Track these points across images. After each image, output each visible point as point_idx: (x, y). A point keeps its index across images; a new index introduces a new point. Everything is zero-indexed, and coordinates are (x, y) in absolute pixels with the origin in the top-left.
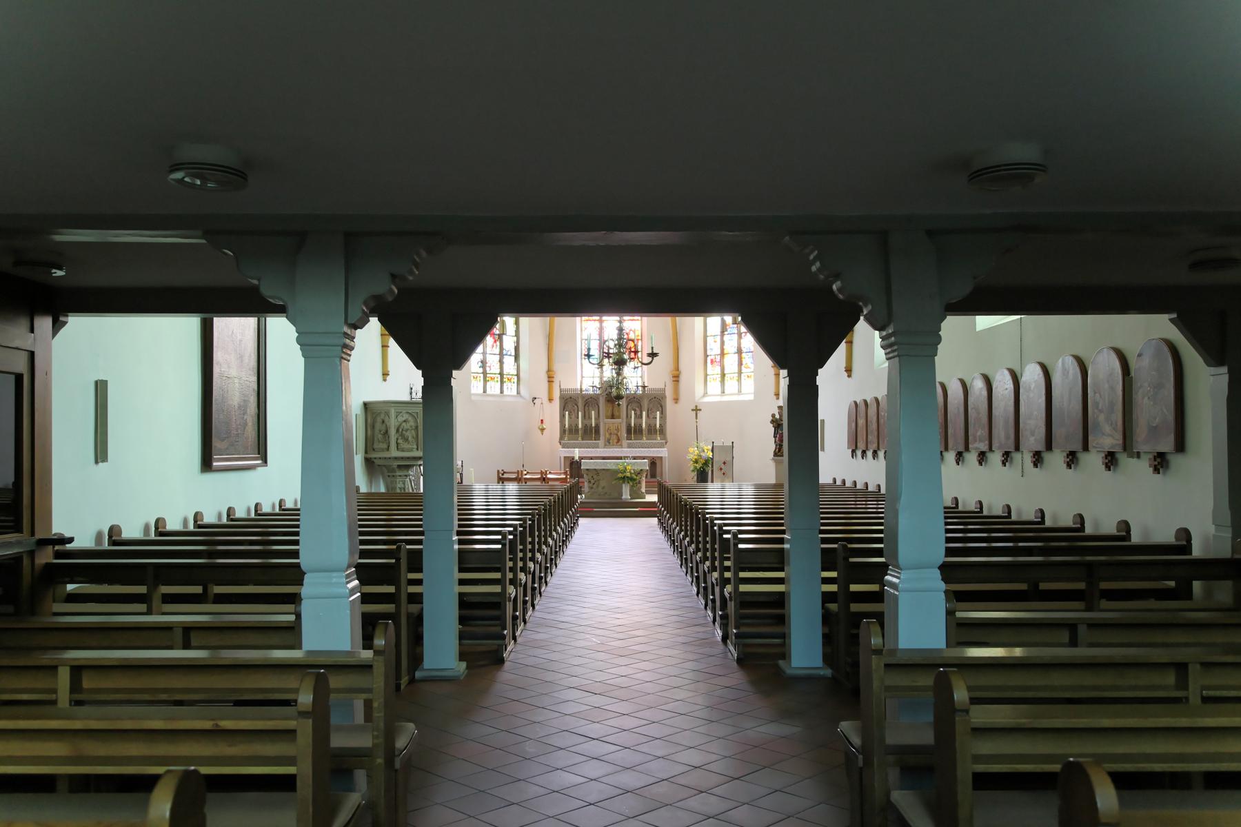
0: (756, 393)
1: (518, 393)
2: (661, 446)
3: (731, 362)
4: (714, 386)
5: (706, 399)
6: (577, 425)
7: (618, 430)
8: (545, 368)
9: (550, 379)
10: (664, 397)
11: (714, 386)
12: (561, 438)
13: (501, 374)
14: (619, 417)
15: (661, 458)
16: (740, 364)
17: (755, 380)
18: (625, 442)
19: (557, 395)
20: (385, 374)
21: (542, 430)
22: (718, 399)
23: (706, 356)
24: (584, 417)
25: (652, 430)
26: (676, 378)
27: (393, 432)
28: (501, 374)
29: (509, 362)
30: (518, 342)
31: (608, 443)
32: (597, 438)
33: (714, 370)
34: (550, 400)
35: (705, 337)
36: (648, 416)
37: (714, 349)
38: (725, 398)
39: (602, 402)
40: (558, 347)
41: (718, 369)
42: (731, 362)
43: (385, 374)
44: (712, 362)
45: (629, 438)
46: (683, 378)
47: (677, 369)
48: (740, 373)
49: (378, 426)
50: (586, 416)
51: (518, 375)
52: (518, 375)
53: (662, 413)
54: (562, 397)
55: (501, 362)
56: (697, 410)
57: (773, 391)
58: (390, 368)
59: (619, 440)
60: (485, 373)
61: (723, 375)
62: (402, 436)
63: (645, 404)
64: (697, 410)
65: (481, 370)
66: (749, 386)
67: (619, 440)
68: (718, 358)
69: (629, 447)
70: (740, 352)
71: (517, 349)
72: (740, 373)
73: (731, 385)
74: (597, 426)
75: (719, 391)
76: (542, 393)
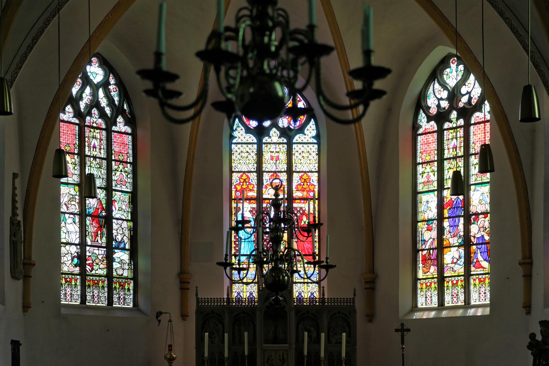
0: (492, 305)
1: (135, 305)
3: (452, 256)
5: (417, 315)
6: (222, 353)
8: (176, 269)
10: (352, 311)
11: (427, 299)
13: (109, 276)
14: (285, 341)
16: (468, 262)
17: (490, 284)
23: (416, 251)
24: (232, 342)
26: (371, 284)
28: (109, 276)
29: (122, 256)
33: (426, 273)
34: (184, 316)
35: (415, 222)
36: (328, 340)
38: (444, 314)
39: (259, 317)
41: (433, 270)
42: (452, 256)
46: (382, 286)
47: (372, 269)
48: (468, 275)
50: (236, 341)
51: (135, 279)
53: (348, 336)
54: (199, 311)
56: (403, 330)
57: (520, 300)
60: (83, 274)
61: (441, 279)
65: (77, 270)
66: (481, 295)
68: (434, 253)
70: (467, 243)
71: (133, 239)
72: (468, 275)
73: (453, 297)
75: (435, 302)
76: (171, 304)
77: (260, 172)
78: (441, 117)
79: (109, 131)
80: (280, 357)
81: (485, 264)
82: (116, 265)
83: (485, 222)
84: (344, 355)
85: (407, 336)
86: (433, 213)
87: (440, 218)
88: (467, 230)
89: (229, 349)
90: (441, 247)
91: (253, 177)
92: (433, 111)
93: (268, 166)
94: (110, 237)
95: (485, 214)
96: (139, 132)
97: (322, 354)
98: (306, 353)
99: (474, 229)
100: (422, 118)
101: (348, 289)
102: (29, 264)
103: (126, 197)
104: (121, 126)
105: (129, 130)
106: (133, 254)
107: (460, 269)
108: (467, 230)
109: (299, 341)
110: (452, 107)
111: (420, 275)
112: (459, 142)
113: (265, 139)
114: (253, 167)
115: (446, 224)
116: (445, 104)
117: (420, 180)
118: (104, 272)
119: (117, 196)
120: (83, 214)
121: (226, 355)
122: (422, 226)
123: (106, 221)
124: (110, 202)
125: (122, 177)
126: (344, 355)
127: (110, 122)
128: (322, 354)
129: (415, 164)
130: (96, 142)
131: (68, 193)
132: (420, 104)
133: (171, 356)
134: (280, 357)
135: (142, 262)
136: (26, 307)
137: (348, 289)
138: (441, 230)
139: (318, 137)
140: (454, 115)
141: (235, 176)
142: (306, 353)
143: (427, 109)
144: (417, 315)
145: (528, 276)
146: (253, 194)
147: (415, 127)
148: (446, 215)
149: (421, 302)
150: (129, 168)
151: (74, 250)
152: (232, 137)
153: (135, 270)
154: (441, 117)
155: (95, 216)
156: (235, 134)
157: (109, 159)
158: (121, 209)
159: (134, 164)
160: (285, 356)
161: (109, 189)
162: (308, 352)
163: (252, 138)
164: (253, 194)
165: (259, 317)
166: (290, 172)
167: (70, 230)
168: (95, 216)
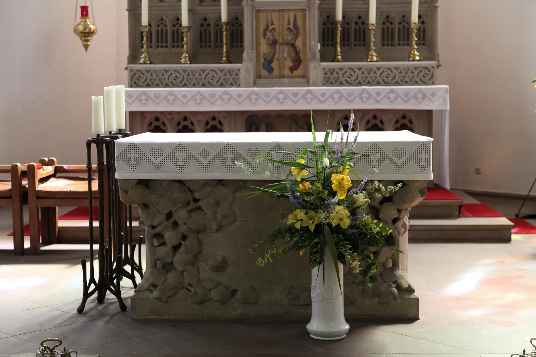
2: (427, 77)
7: (295, 30)
12: (133, 58)
15: (429, 113)
18: (317, 68)
21: (86, 35)
25: (397, 34)
31: (267, 71)
32: (235, 56)
45: (328, 55)
59: (297, 62)
67: (297, 62)
69: (330, 79)
74: (236, 23)
80: (289, 24)
84: (415, 18)
89: (190, 10)
97: (373, 18)
98: (339, 16)
121: (185, 21)
126: (415, 18)
128: (373, 18)
133: (86, 26)
134: (289, 24)
142: (339, 16)
160: (299, 23)
162: (344, 17)
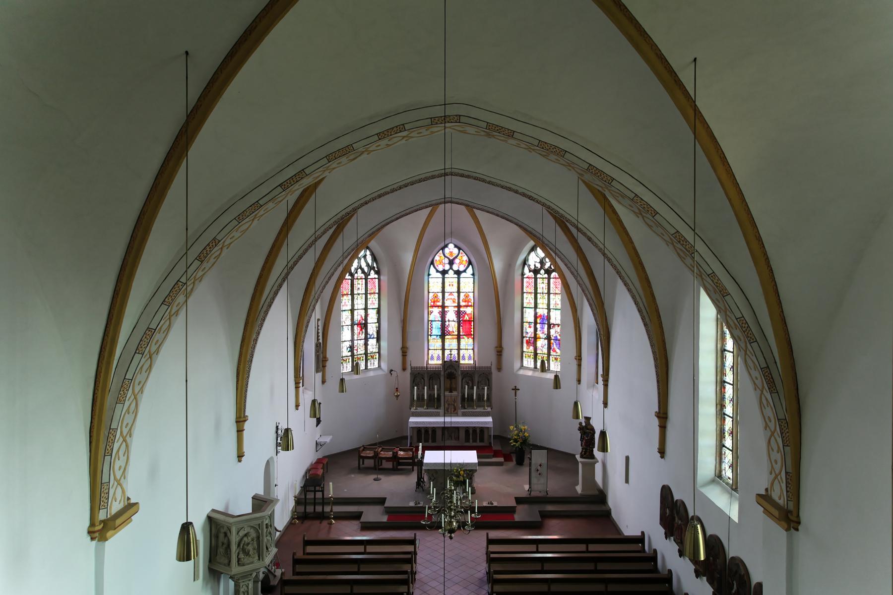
1: (379, 366)
3: (542, 343)
4: (528, 362)
5: (521, 372)
7: (455, 401)
8: (400, 346)
9: (404, 352)
10: (490, 373)
12: (411, 405)
14: (455, 389)
16: (549, 348)
18: (461, 411)
19: (409, 371)
20: (240, 456)
22: (530, 373)
23: (523, 337)
24: (429, 389)
26: (499, 351)
27: (234, 547)
28: (366, 354)
29: (372, 342)
30: (379, 327)
33: (528, 350)
34: (404, 369)
35: (522, 322)
36: (478, 388)
37: (530, 331)
40: (412, 329)
41: (532, 348)
42: (542, 343)
43: (240, 456)
44: (528, 342)
46: (505, 354)
49: (221, 536)
50: (431, 389)
51: (379, 352)
52: (379, 352)
55: (366, 345)
56: (516, 389)
57: (575, 377)
58: (246, 449)
59: (455, 409)
60: (353, 356)
62: (244, 550)
63: (476, 379)
64: (516, 389)
65: (350, 354)
67: (455, 409)
70: (549, 338)
71: (378, 332)
75: (532, 366)
77: (443, 292)
78: (536, 272)
79: (366, 279)
81: (558, 350)
82: (369, 347)
83: (558, 329)
85: (518, 392)
86: (532, 320)
87: (536, 323)
88: (549, 332)
90: (536, 338)
91: (440, 295)
92: (532, 267)
93: (447, 289)
94: (366, 333)
95: (558, 325)
96: (382, 278)
99: (552, 332)
100: (526, 270)
101: (490, 360)
102: (325, 360)
103: (375, 311)
104: (373, 275)
105: (376, 276)
106: (378, 339)
107: (545, 351)
108: (549, 332)
109: (463, 388)
110: (542, 268)
111: (525, 349)
112: (545, 286)
113: (446, 276)
114: (440, 289)
115: (538, 326)
116: (538, 266)
117: (525, 301)
118: (363, 352)
119: (369, 311)
120: (352, 325)
122: (526, 325)
123: (364, 325)
124: (366, 315)
125: (373, 301)
127: (367, 275)
129: (523, 293)
130: (360, 286)
131: (346, 318)
132: (525, 263)
135: (384, 344)
136: (323, 382)
137: (490, 360)
138: (536, 329)
139: (473, 274)
140: (542, 272)
141: (431, 295)
143: (529, 266)
144: (521, 372)
145: (579, 365)
146: (440, 304)
147: (523, 274)
148: (539, 321)
149: (525, 364)
150: (377, 296)
151: (348, 344)
152: (429, 275)
153: (379, 348)
154: (536, 272)
155: (359, 324)
156: (431, 272)
157: (366, 294)
158: (372, 316)
159: (379, 294)
161: (366, 309)
163: (440, 275)
164: (440, 304)
165: (442, 379)
166: (459, 292)
167: (346, 335)
168: (359, 324)
